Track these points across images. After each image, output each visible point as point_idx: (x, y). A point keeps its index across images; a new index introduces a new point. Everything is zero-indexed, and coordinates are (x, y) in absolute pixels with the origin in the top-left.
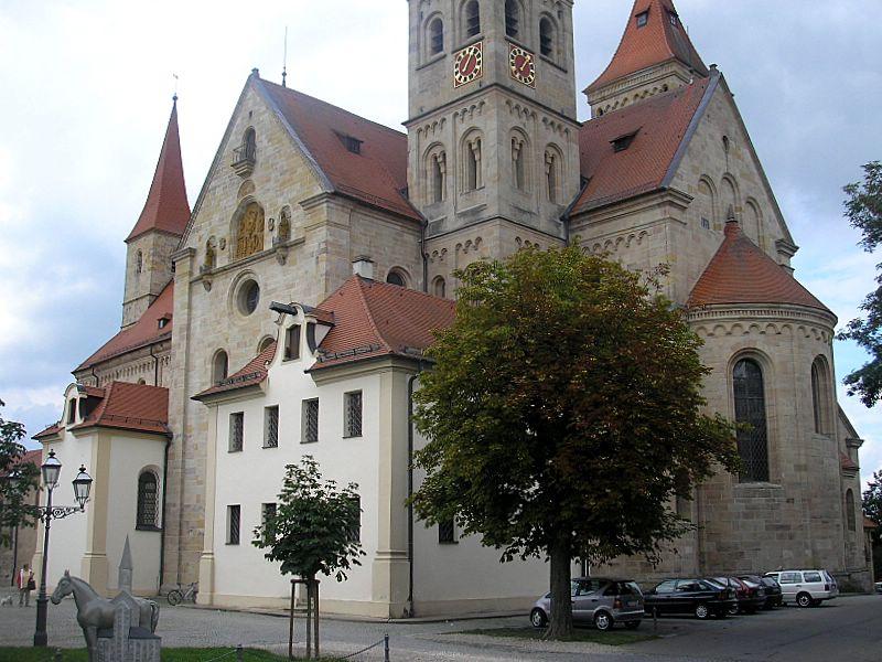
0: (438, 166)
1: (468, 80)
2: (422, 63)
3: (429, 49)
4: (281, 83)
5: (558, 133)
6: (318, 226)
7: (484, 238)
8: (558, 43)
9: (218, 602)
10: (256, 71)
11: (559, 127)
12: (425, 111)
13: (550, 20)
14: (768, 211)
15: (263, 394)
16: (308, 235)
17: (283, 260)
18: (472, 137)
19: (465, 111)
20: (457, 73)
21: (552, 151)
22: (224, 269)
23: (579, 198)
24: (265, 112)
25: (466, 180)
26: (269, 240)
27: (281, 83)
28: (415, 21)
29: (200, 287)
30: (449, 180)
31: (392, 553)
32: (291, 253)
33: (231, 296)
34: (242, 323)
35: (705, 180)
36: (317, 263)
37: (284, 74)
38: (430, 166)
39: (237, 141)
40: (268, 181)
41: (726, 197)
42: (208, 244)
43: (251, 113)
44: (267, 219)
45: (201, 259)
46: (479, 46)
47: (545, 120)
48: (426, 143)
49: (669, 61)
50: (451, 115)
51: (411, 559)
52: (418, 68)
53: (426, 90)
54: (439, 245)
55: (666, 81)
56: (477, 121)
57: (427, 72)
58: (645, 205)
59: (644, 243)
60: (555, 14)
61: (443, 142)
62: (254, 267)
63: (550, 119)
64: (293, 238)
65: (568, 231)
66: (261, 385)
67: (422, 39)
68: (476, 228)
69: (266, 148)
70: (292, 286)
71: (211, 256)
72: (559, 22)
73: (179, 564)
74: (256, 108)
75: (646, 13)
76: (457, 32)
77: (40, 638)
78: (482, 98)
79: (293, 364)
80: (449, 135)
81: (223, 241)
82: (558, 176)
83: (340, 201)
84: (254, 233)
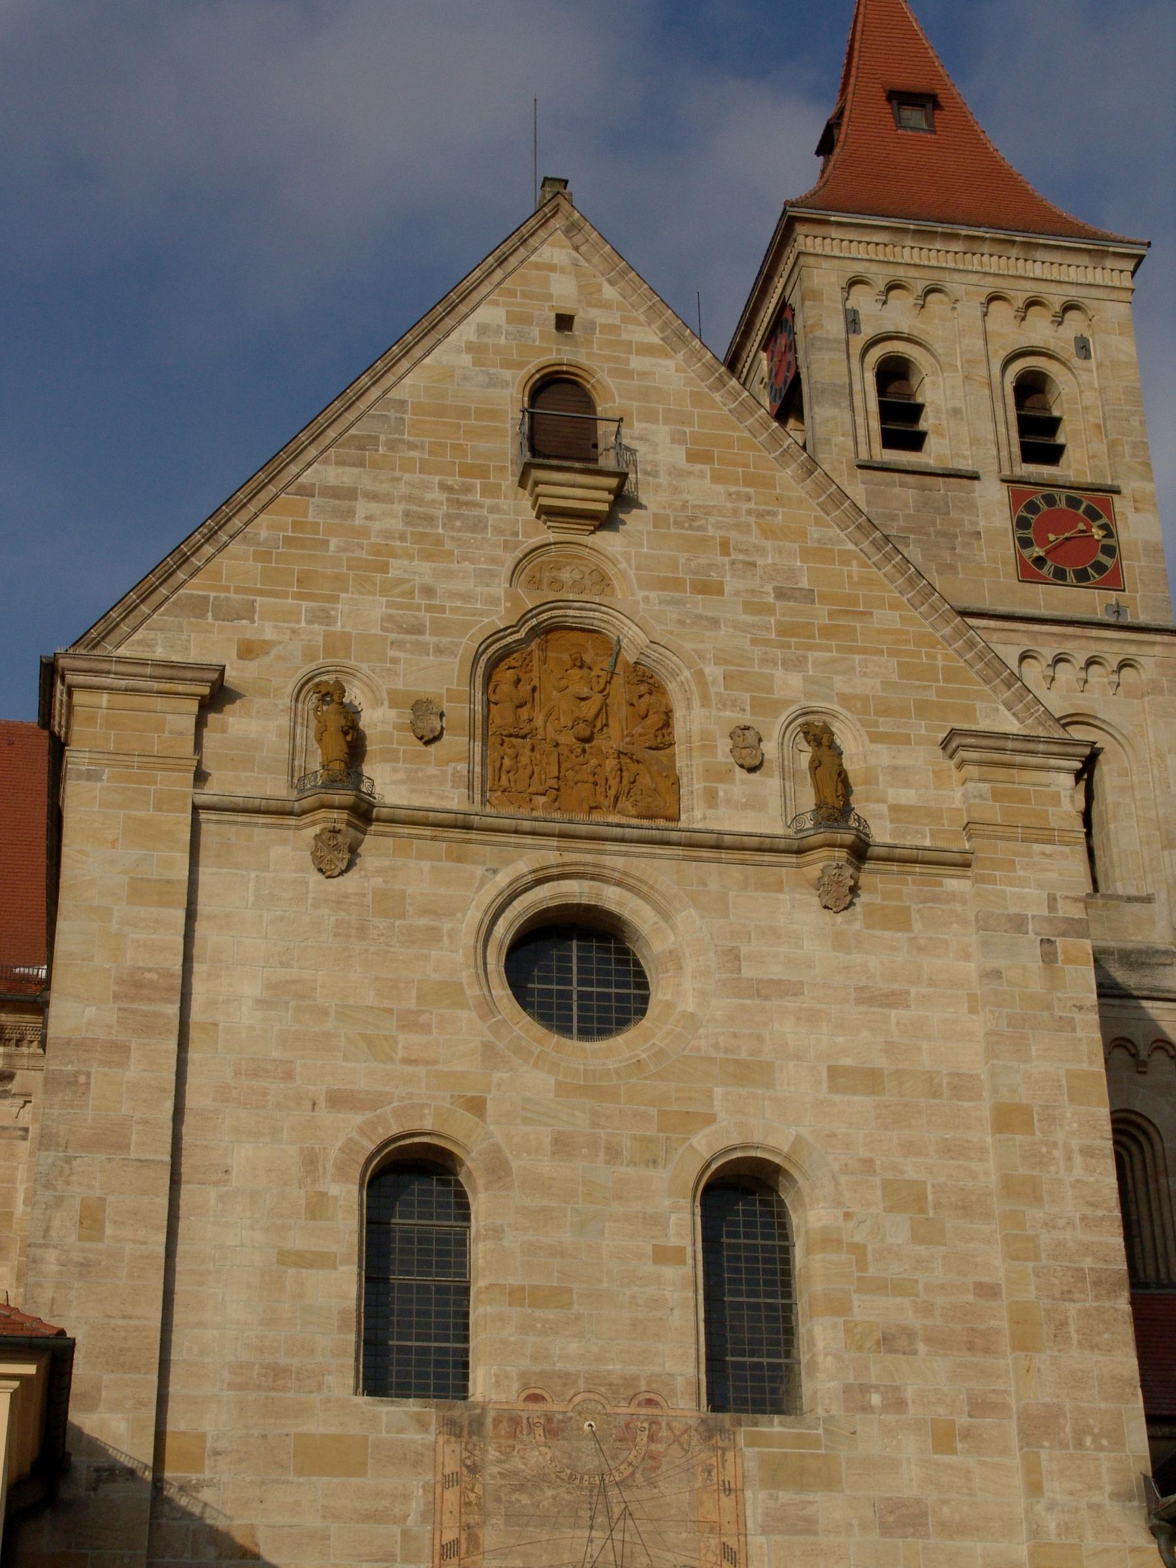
2: (864, 456)
24: (646, 350)
29: (288, 851)
40: (708, 588)
42: (327, 695)
43: (564, 322)
45: (262, 741)
62: (660, 869)
70: (894, 999)
74: (600, 316)
78: (1131, 650)
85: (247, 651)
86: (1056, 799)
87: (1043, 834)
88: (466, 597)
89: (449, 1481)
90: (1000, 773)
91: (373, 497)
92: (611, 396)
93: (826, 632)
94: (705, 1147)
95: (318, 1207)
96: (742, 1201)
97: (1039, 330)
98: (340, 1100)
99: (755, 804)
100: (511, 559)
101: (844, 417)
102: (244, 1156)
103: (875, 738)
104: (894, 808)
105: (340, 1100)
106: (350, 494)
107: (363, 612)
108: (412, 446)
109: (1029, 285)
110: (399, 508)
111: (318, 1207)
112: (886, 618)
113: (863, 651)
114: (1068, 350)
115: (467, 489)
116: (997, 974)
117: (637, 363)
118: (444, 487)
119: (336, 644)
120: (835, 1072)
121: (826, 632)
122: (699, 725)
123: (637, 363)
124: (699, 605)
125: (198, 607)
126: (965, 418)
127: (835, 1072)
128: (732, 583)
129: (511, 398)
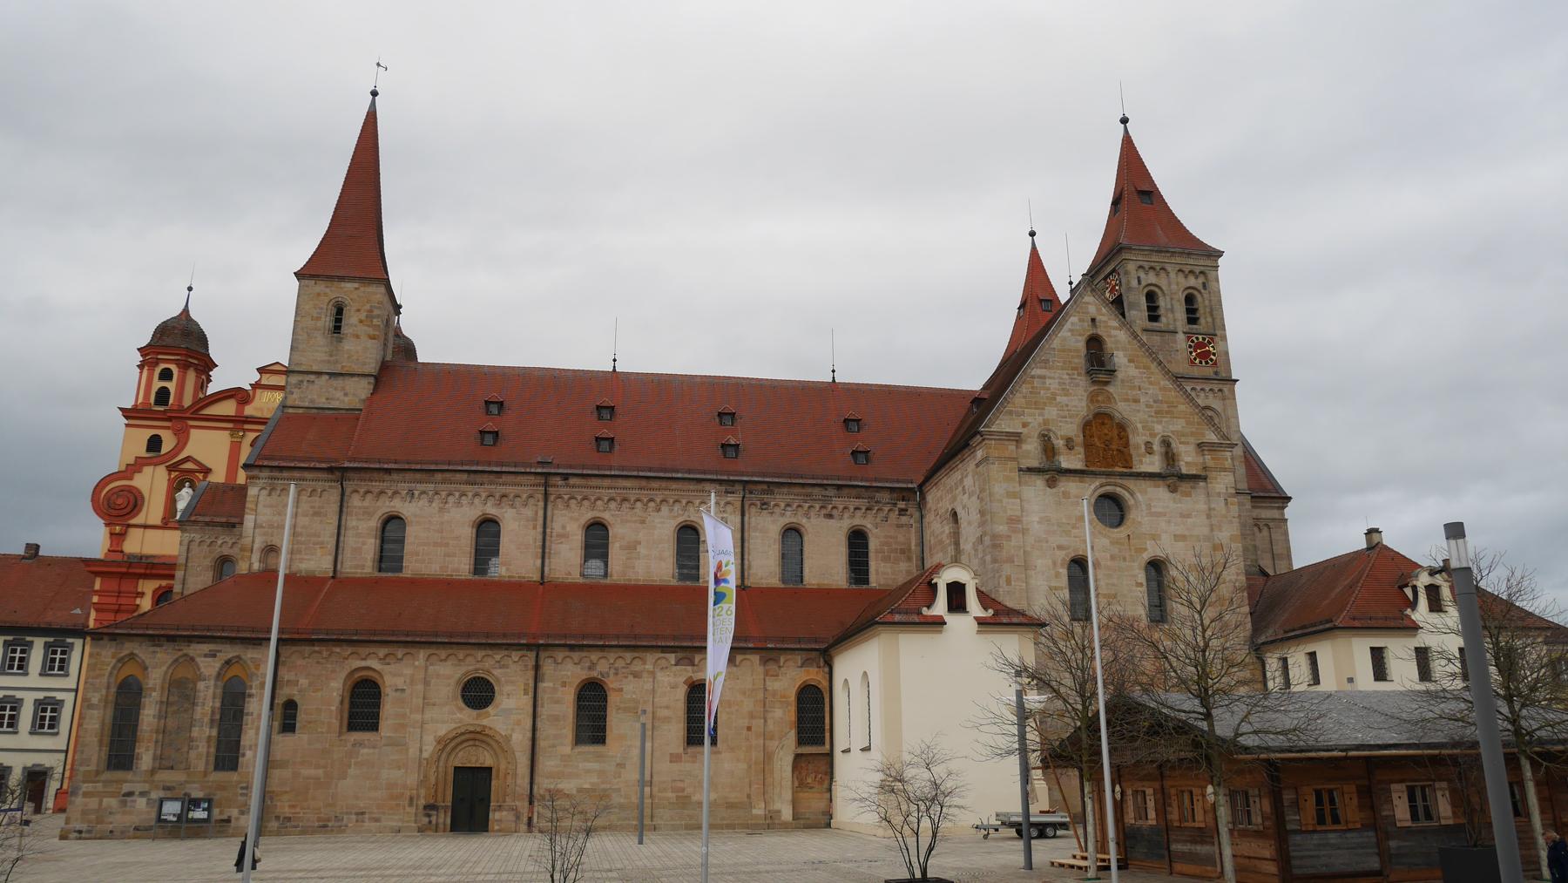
16: (1212, 475)
40: (1136, 401)
43: (1093, 320)
45: (1031, 452)
62: (1131, 483)
70: (1189, 516)
71: (1049, 450)
85: (1025, 425)
87: (1225, 470)
92: (1109, 344)
94: (1146, 556)
95: (1057, 575)
97: (1192, 281)
98: (1060, 547)
99: (1152, 463)
101: (1139, 314)
102: (1039, 562)
105: (1060, 547)
106: (1044, 377)
107: (1051, 412)
111: (1057, 575)
112: (1182, 407)
114: (1200, 287)
119: (1046, 422)
122: (1137, 439)
123: (1114, 332)
124: (1134, 406)
125: (1011, 413)
126: (1173, 314)
129: (1081, 345)
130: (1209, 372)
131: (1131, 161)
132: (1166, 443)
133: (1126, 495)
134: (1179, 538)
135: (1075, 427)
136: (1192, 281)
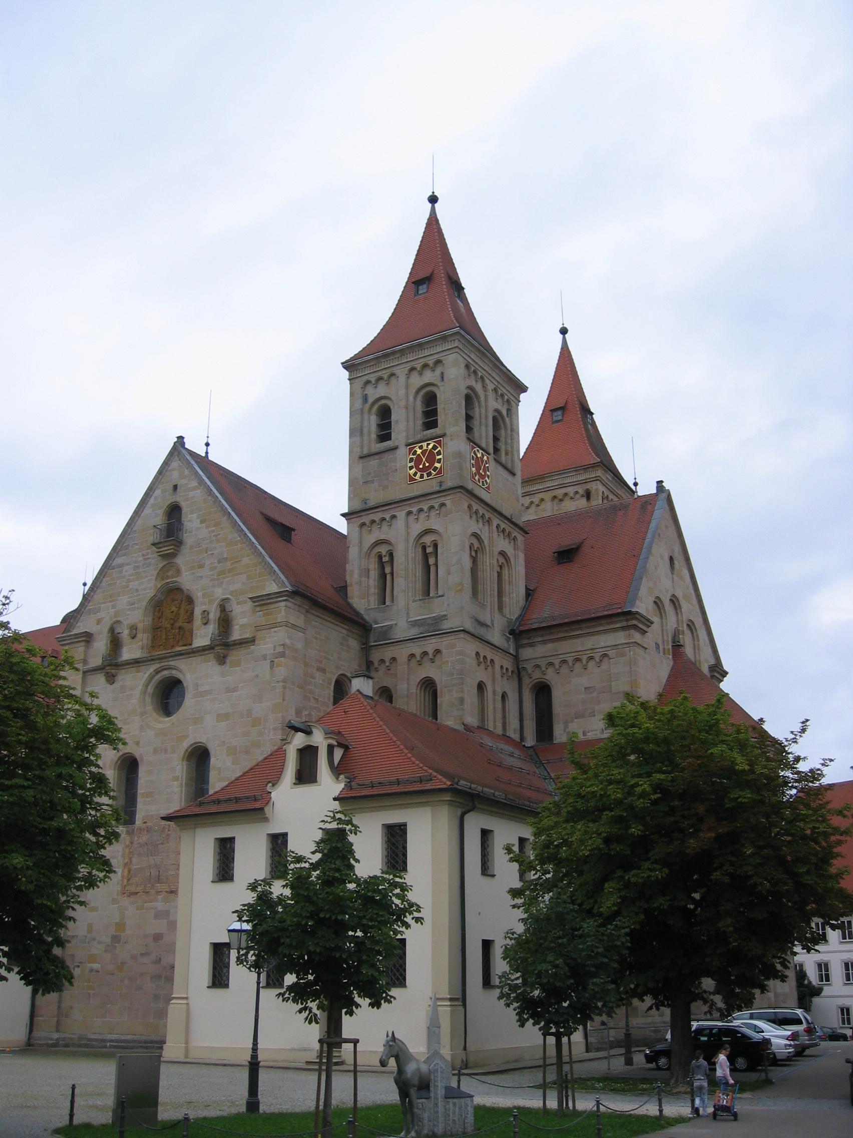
0: (382, 565)
1: (425, 477)
2: (366, 452)
3: (374, 436)
4: (203, 455)
5: (507, 541)
6: (275, 625)
7: (444, 651)
8: (506, 443)
9: (195, 1055)
10: (181, 438)
11: (509, 534)
12: (372, 503)
13: (499, 418)
14: (702, 634)
15: (266, 819)
16: (259, 635)
17: (222, 660)
18: (428, 540)
19: (421, 510)
20: (411, 468)
21: (502, 560)
22: (136, 662)
23: (525, 610)
24: (194, 488)
25: (419, 585)
26: (203, 636)
27: (203, 455)
28: (358, 404)
30: (400, 583)
31: (451, 1000)
32: (235, 652)
33: (144, 692)
34: (160, 726)
35: (658, 603)
36: (272, 667)
37: (207, 444)
38: (373, 566)
39: (156, 517)
40: (201, 566)
41: (672, 620)
42: (112, 630)
43: (175, 487)
44: (198, 612)
45: (101, 646)
46: (439, 443)
47: (498, 527)
48: (370, 539)
49: (593, 466)
50: (404, 513)
51: (464, 1005)
52: (361, 457)
53: (372, 482)
54: (388, 653)
55: (588, 486)
56: (435, 523)
57: (374, 462)
58: (608, 627)
59: (604, 666)
60: (504, 412)
61: (393, 541)
63: (503, 526)
64: (236, 635)
65: (518, 647)
66: (266, 809)
67: (366, 424)
68: (434, 640)
69: (198, 529)
70: (234, 690)
71: (116, 643)
72: (507, 420)
73: (59, 1007)
74: (183, 482)
75: (563, 409)
76: (411, 423)
77: (253, 1105)
78: (442, 500)
79: (306, 790)
80: (401, 533)
81: (134, 629)
82: (506, 586)
83: (298, 600)
84: (178, 624)
86: (280, 612)
88: (145, 589)
89: (128, 846)
90: (265, 607)
91: (128, 564)
93: (229, 571)
96: (199, 757)
97: (429, 376)
100: (155, 573)
103: (238, 603)
104: (242, 626)
106: (121, 566)
108: (136, 544)
109: (421, 360)
110: (132, 566)
112: (246, 560)
113: (239, 574)
115: (148, 554)
116: (257, 676)
117: (191, 494)
118: (143, 555)
120: (218, 716)
121: (229, 571)
127: (218, 716)
128: (207, 562)
130: (432, 485)
131: (433, 242)
132: (223, 608)
133: (181, 677)
134: (221, 717)
135: (141, 611)
136: (429, 376)
